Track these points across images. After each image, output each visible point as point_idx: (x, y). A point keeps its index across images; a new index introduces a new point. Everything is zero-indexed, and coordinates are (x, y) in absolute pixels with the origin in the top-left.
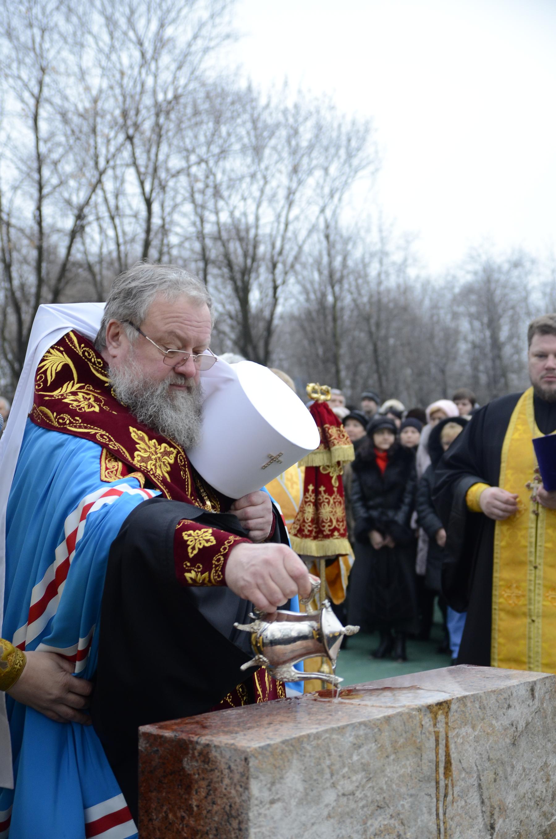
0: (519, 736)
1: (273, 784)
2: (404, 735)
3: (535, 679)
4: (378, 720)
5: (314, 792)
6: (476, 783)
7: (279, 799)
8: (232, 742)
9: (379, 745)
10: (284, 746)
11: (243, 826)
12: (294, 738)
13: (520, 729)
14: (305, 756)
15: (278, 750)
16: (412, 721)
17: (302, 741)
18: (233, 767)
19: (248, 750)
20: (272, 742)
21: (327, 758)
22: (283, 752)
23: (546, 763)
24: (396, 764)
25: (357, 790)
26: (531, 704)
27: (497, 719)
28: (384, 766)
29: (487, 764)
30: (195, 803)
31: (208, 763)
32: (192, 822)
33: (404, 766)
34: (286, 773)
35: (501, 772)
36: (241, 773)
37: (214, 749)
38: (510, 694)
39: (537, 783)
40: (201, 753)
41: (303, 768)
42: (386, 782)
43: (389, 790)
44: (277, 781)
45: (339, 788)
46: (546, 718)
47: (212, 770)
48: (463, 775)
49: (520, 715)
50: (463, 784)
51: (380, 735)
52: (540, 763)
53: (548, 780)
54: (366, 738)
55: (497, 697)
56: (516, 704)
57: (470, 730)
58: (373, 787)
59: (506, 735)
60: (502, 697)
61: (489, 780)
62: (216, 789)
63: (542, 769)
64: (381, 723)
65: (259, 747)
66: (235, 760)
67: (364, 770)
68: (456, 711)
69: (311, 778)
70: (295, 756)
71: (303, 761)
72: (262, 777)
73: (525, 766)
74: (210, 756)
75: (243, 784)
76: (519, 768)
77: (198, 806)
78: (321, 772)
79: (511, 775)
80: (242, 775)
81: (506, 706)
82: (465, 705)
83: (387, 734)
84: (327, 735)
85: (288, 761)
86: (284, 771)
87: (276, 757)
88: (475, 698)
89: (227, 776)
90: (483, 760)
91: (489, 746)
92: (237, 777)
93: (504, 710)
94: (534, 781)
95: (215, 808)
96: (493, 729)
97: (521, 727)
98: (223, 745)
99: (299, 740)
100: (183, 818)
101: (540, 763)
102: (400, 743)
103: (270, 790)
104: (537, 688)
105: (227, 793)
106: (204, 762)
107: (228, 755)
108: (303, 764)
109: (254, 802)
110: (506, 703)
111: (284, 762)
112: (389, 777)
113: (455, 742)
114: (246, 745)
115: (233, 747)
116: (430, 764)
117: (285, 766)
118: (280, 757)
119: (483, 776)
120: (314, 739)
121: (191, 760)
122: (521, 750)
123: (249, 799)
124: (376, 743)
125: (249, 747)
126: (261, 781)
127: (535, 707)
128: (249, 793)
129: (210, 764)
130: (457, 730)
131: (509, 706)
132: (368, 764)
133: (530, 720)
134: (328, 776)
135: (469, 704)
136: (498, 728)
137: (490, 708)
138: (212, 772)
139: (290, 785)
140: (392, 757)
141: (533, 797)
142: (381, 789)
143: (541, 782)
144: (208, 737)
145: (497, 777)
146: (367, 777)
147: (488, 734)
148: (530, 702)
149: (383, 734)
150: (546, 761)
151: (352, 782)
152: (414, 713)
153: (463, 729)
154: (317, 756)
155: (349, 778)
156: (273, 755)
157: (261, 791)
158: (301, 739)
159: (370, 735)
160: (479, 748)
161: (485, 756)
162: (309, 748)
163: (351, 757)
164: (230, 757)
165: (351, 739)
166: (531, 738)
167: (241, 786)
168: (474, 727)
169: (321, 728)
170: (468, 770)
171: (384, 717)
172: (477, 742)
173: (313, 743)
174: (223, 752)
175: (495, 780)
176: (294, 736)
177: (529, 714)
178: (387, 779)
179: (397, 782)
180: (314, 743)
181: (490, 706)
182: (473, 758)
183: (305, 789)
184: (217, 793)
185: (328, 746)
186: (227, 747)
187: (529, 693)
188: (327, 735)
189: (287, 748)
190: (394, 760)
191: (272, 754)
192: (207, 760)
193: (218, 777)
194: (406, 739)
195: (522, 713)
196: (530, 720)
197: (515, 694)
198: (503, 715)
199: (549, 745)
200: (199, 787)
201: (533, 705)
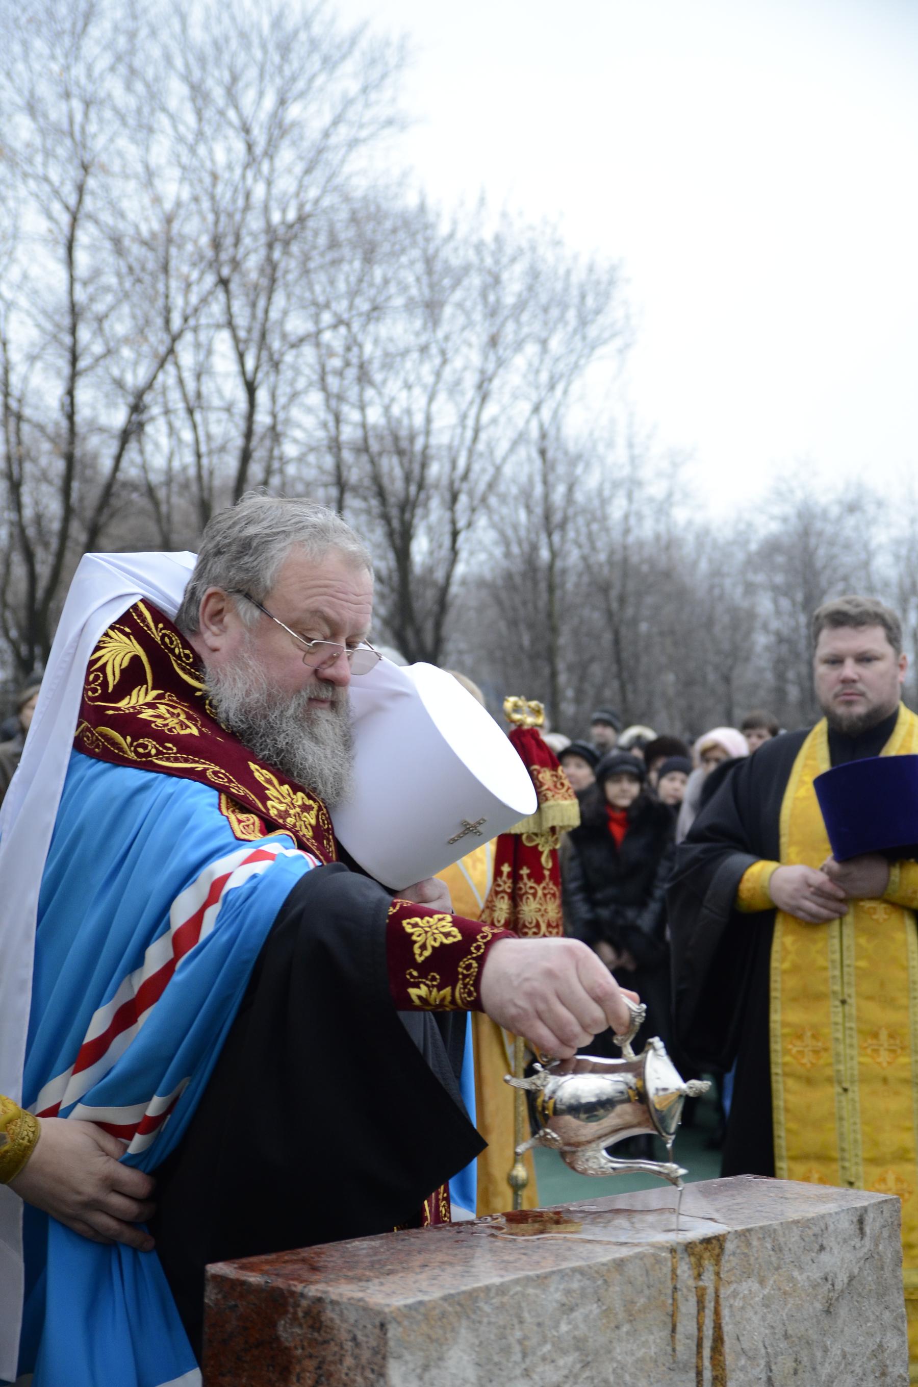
0: (837, 1299)
1: (426, 1368)
2: (647, 1292)
3: (866, 1204)
4: (603, 1264)
5: (494, 1383)
6: (763, 1376)
8: (360, 1295)
9: (604, 1308)
10: (446, 1305)
12: (464, 1292)
13: (839, 1286)
14: (480, 1322)
15: (437, 1311)
16: (660, 1269)
17: (477, 1297)
18: (360, 1337)
19: (387, 1310)
20: (426, 1298)
21: (517, 1327)
22: (443, 1315)
23: (880, 1346)
24: (631, 1341)
25: (565, 1382)
26: (858, 1245)
27: (801, 1268)
28: (611, 1342)
29: (783, 1345)
31: (319, 1330)
33: (645, 1344)
34: (448, 1350)
35: (805, 1359)
36: (373, 1348)
37: (329, 1307)
38: (823, 1227)
39: (865, 1378)
40: (307, 1313)
41: (477, 1342)
42: (614, 1370)
43: (618, 1384)
44: (432, 1363)
45: (536, 1377)
46: (882, 1269)
47: (326, 1342)
48: (743, 1362)
49: (839, 1263)
50: (742, 1376)
51: (606, 1290)
52: (871, 1345)
53: (884, 1374)
54: (583, 1294)
55: (802, 1232)
56: (833, 1244)
57: (756, 1286)
58: (592, 1378)
59: (816, 1295)
60: (810, 1232)
61: (786, 1371)
62: (330, 1375)
63: (874, 1354)
64: (609, 1271)
65: (405, 1306)
66: (365, 1327)
67: (578, 1349)
68: (734, 1254)
69: (489, 1360)
70: (464, 1323)
71: (477, 1330)
72: (408, 1357)
73: (846, 1349)
74: (323, 1319)
75: (376, 1368)
76: (836, 1351)
78: (506, 1351)
79: (822, 1364)
80: (376, 1351)
81: (817, 1247)
82: (749, 1244)
83: (617, 1289)
84: (519, 1288)
85: (453, 1330)
86: (445, 1348)
87: (433, 1322)
88: (766, 1232)
89: (349, 1353)
90: (777, 1337)
91: (787, 1314)
92: (366, 1355)
93: (813, 1255)
94: (860, 1375)
96: (794, 1285)
97: (841, 1283)
98: (345, 1300)
99: (472, 1295)
101: (871, 1345)
102: (638, 1304)
103: (420, 1378)
104: (869, 1218)
105: (349, 1382)
106: (312, 1327)
107: (352, 1316)
108: (477, 1336)
110: (817, 1243)
111: (445, 1333)
112: (618, 1362)
113: (731, 1306)
114: (383, 1301)
115: (361, 1304)
116: (688, 1341)
117: (446, 1339)
118: (439, 1323)
119: (776, 1363)
120: (497, 1294)
121: (291, 1325)
122: (840, 1322)
124: (600, 1303)
125: (388, 1305)
126: (406, 1362)
127: (865, 1250)
128: (386, 1383)
129: (322, 1332)
130: (734, 1286)
131: (822, 1248)
132: (585, 1339)
133: (856, 1271)
134: (517, 1357)
135: (755, 1243)
136: (802, 1283)
137: (790, 1249)
138: (325, 1346)
139: (454, 1371)
140: (625, 1328)
142: (606, 1381)
143: (873, 1377)
144: (321, 1287)
145: (800, 1367)
146: (581, 1361)
147: (785, 1293)
148: (856, 1242)
149: (611, 1289)
150: (881, 1342)
151: (557, 1368)
152: (663, 1254)
153: (744, 1283)
154: (501, 1323)
155: (553, 1361)
156: (427, 1319)
157: (405, 1380)
158: (475, 1294)
159: (590, 1290)
160: (769, 1316)
161: (779, 1331)
162: (487, 1308)
163: (556, 1327)
164: (356, 1321)
165: (558, 1296)
166: (857, 1301)
167: (373, 1371)
168: (762, 1282)
169: (509, 1277)
170: (751, 1354)
171: (614, 1260)
172: (767, 1306)
173: (494, 1301)
174: (345, 1312)
175: (796, 1372)
176: (463, 1288)
177: (854, 1262)
178: (615, 1365)
179: (633, 1370)
180: (496, 1301)
181: (791, 1246)
182: (760, 1333)
183: (480, 1378)
184: (332, 1380)
185: (520, 1307)
186: (352, 1304)
187: (854, 1228)
188: (519, 1288)
189: (450, 1309)
190: (628, 1333)
191: (426, 1317)
192: (317, 1325)
193: (335, 1354)
194: (649, 1298)
195: (843, 1259)
196: (856, 1271)
197: (831, 1228)
198: (810, 1262)
199: (887, 1315)
200: (304, 1370)
201: (863, 1246)
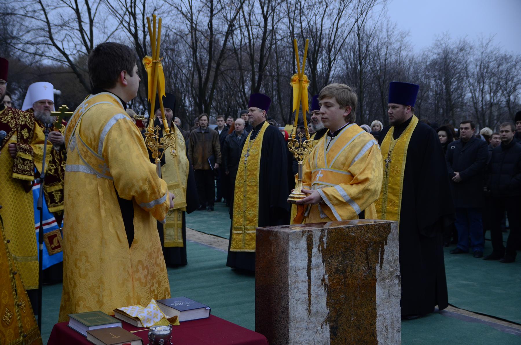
1: (296, 243)
11: (287, 255)
23: (393, 250)
32: (272, 255)
40: (275, 234)
53: (393, 256)
62: (279, 245)
63: (391, 252)
80: (287, 240)
92: (285, 241)
95: (279, 250)
107: (283, 234)
109: (290, 248)
141: (387, 260)
191: (296, 234)
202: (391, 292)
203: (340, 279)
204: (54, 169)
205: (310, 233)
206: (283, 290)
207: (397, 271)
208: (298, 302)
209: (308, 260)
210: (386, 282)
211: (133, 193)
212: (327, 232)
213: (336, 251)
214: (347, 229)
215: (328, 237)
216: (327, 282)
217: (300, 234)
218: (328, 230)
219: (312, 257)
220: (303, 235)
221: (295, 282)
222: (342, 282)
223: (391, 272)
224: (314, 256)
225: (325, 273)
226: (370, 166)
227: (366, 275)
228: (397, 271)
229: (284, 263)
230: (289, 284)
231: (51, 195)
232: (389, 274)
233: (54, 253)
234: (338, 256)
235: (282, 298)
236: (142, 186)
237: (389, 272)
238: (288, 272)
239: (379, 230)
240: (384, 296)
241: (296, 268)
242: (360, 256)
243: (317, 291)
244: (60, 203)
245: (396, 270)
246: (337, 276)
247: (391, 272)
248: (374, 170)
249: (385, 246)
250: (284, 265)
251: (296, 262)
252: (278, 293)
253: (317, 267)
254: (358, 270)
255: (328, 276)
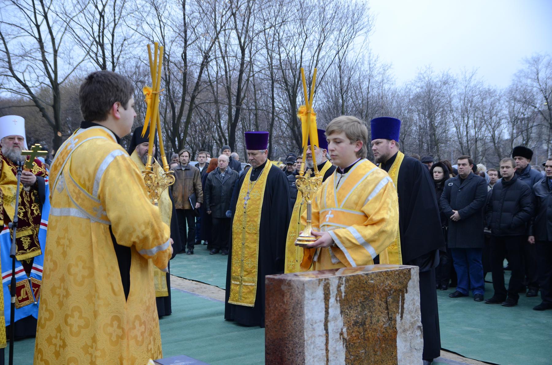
1: (313, 293)
7: (314, 299)
11: (302, 306)
18: (299, 287)
23: (413, 298)
30: (285, 300)
32: (284, 307)
40: (288, 283)
47: (291, 289)
53: (414, 305)
62: (292, 295)
63: (412, 300)
72: (309, 290)
77: (287, 301)
95: (293, 301)
100: (281, 305)
103: (311, 295)
106: (289, 286)
107: (297, 283)
109: (306, 298)
123: (304, 297)
157: (308, 295)
199: (415, 292)
202: (412, 345)
203: (359, 332)
204: (23, 212)
205: (327, 281)
206: (298, 346)
207: (418, 321)
208: (316, 359)
209: (326, 311)
210: (407, 335)
211: (134, 239)
212: (345, 280)
213: (355, 300)
214: (365, 276)
215: (346, 286)
216: (345, 336)
217: (316, 283)
218: (346, 277)
219: (329, 308)
220: (319, 283)
221: (312, 337)
222: (362, 336)
223: (412, 323)
224: (332, 307)
225: (344, 326)
226: (386, 205)
227: (386, 327)
228: (418, 321)
229: (300, 316)
230: (306, 339)
231: (19, 242)
232: (410, 325)
233: (22, 306)
234: (356, 306)
235: (297, 355)
236: (144, 231)
237: (410, 323)
238: (303, 325)
239: (399, 276)
240: (405, 350)
241: (312, 321)
242: (380, 305)
243: (334, 346)
244: (29, 250)
245: (417, 320)
246: (356, 329)
247: (412, 323)
248: (390, 210)
249: (406, 295)
250: (299, 318)
251: (312, 315)
252: (292, 349)
253: (335, 319)
254: (378, 321)
255: (347, 329)
